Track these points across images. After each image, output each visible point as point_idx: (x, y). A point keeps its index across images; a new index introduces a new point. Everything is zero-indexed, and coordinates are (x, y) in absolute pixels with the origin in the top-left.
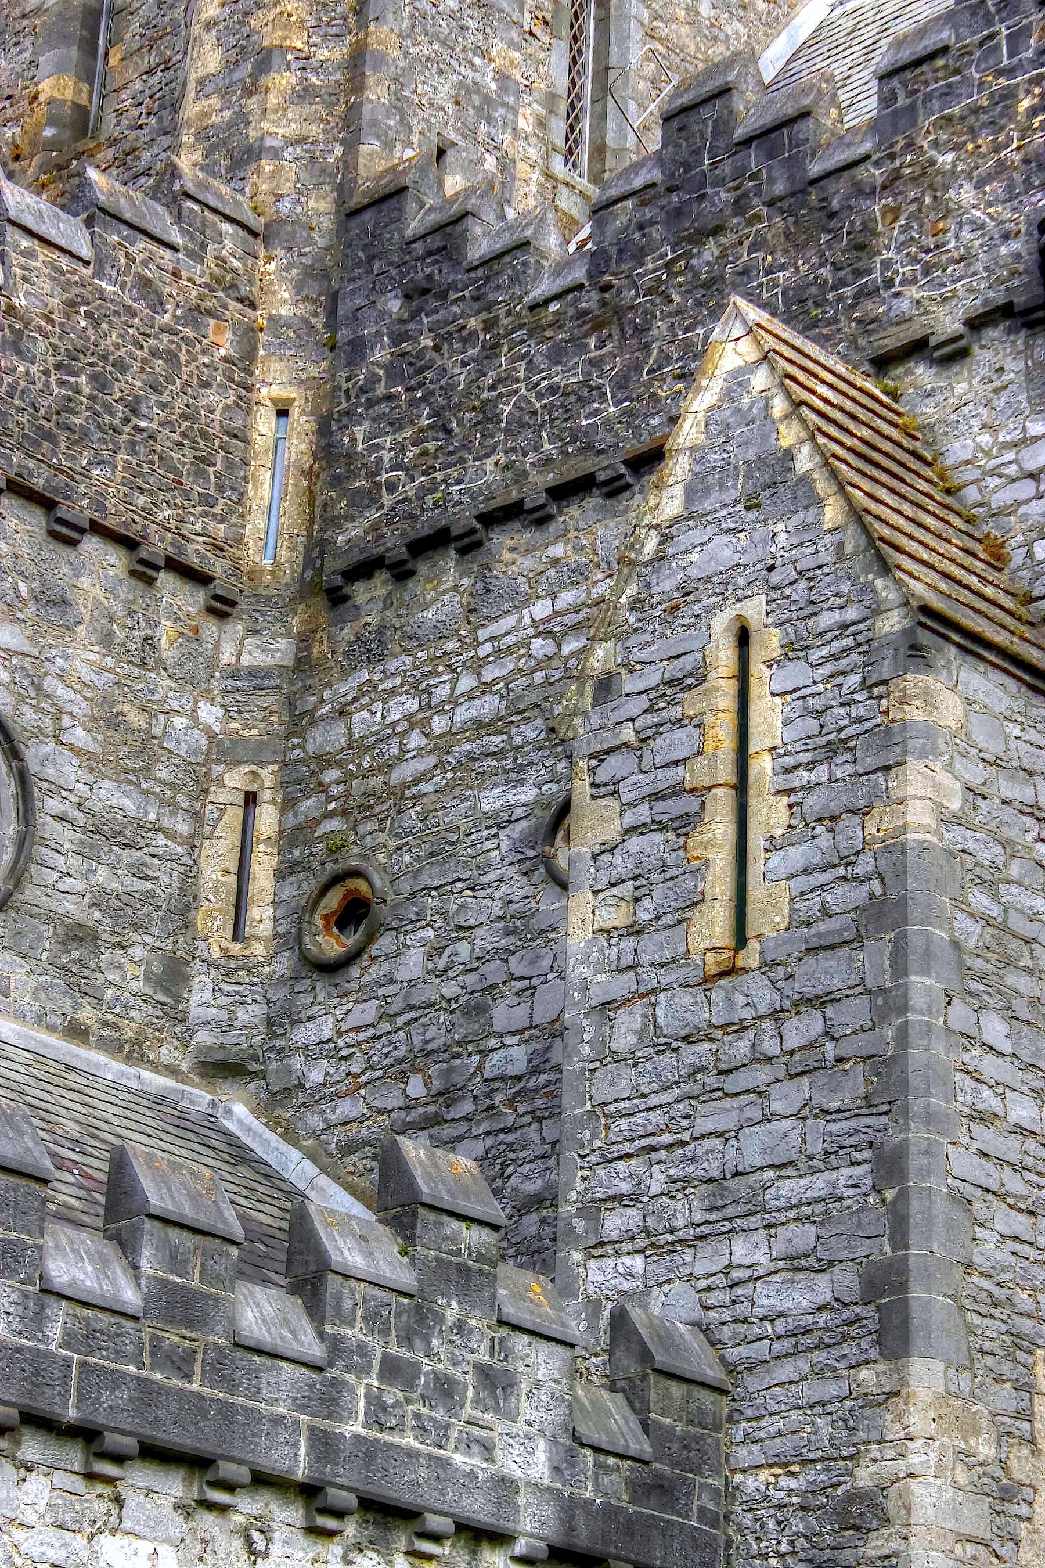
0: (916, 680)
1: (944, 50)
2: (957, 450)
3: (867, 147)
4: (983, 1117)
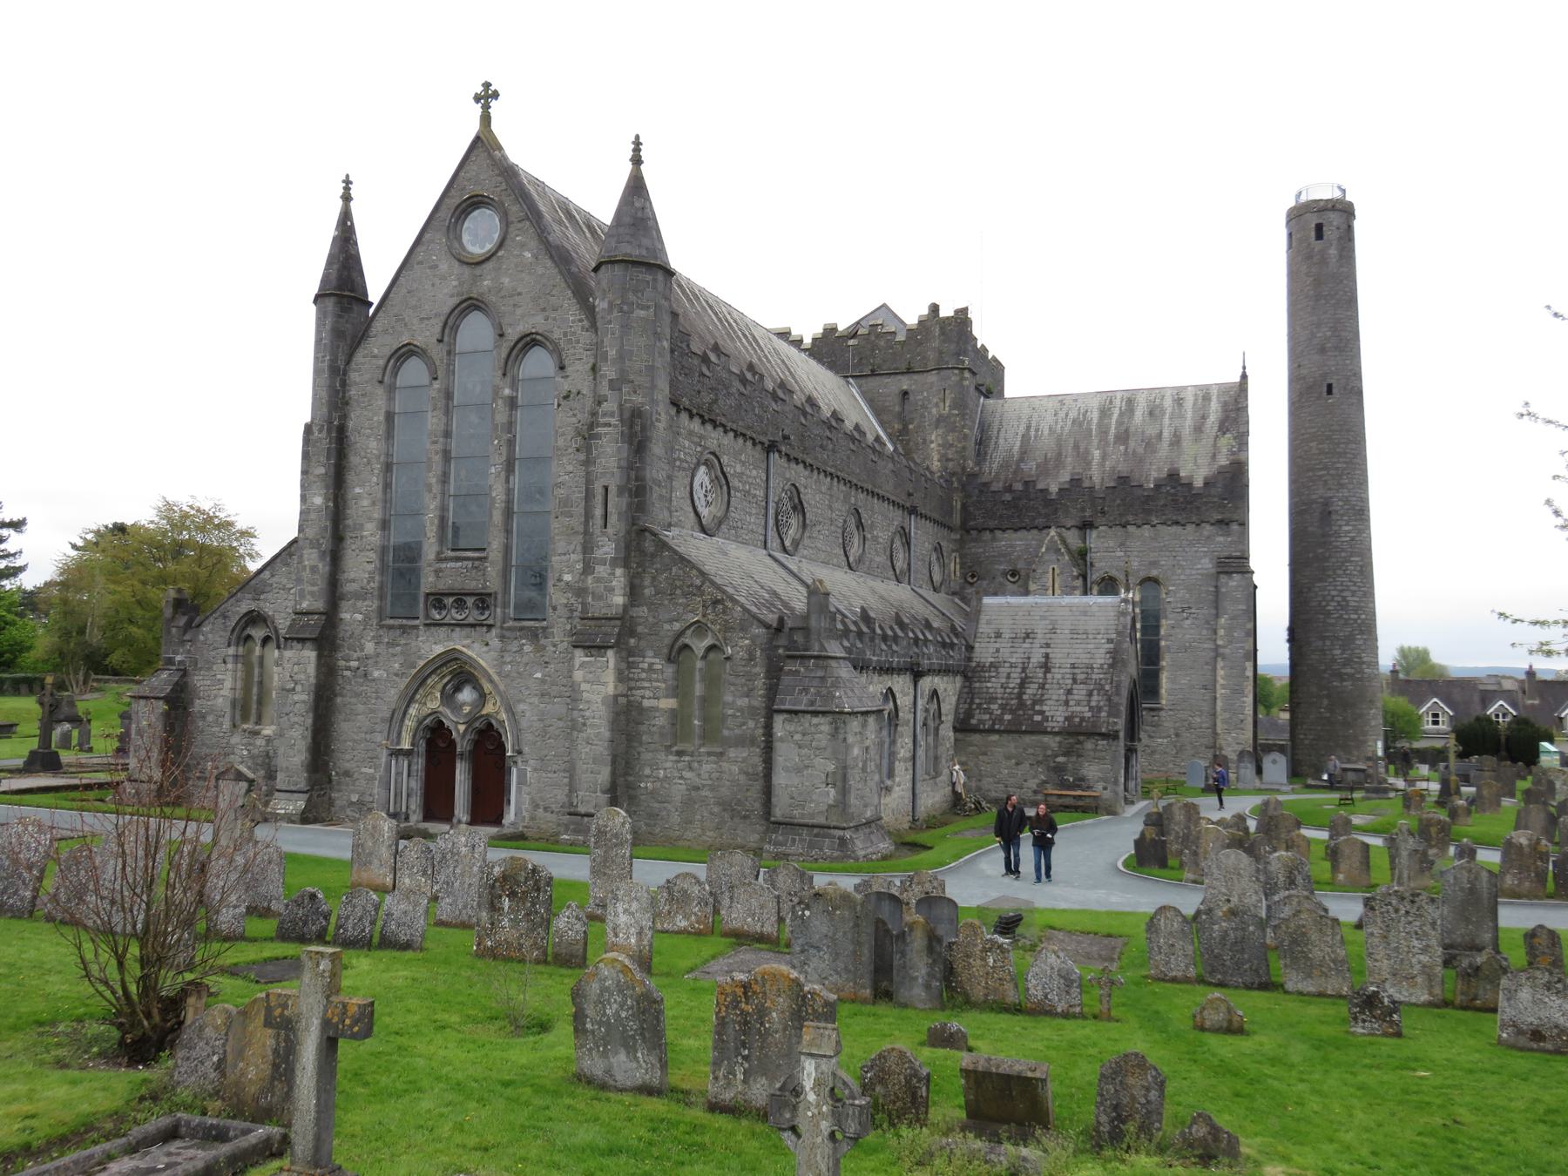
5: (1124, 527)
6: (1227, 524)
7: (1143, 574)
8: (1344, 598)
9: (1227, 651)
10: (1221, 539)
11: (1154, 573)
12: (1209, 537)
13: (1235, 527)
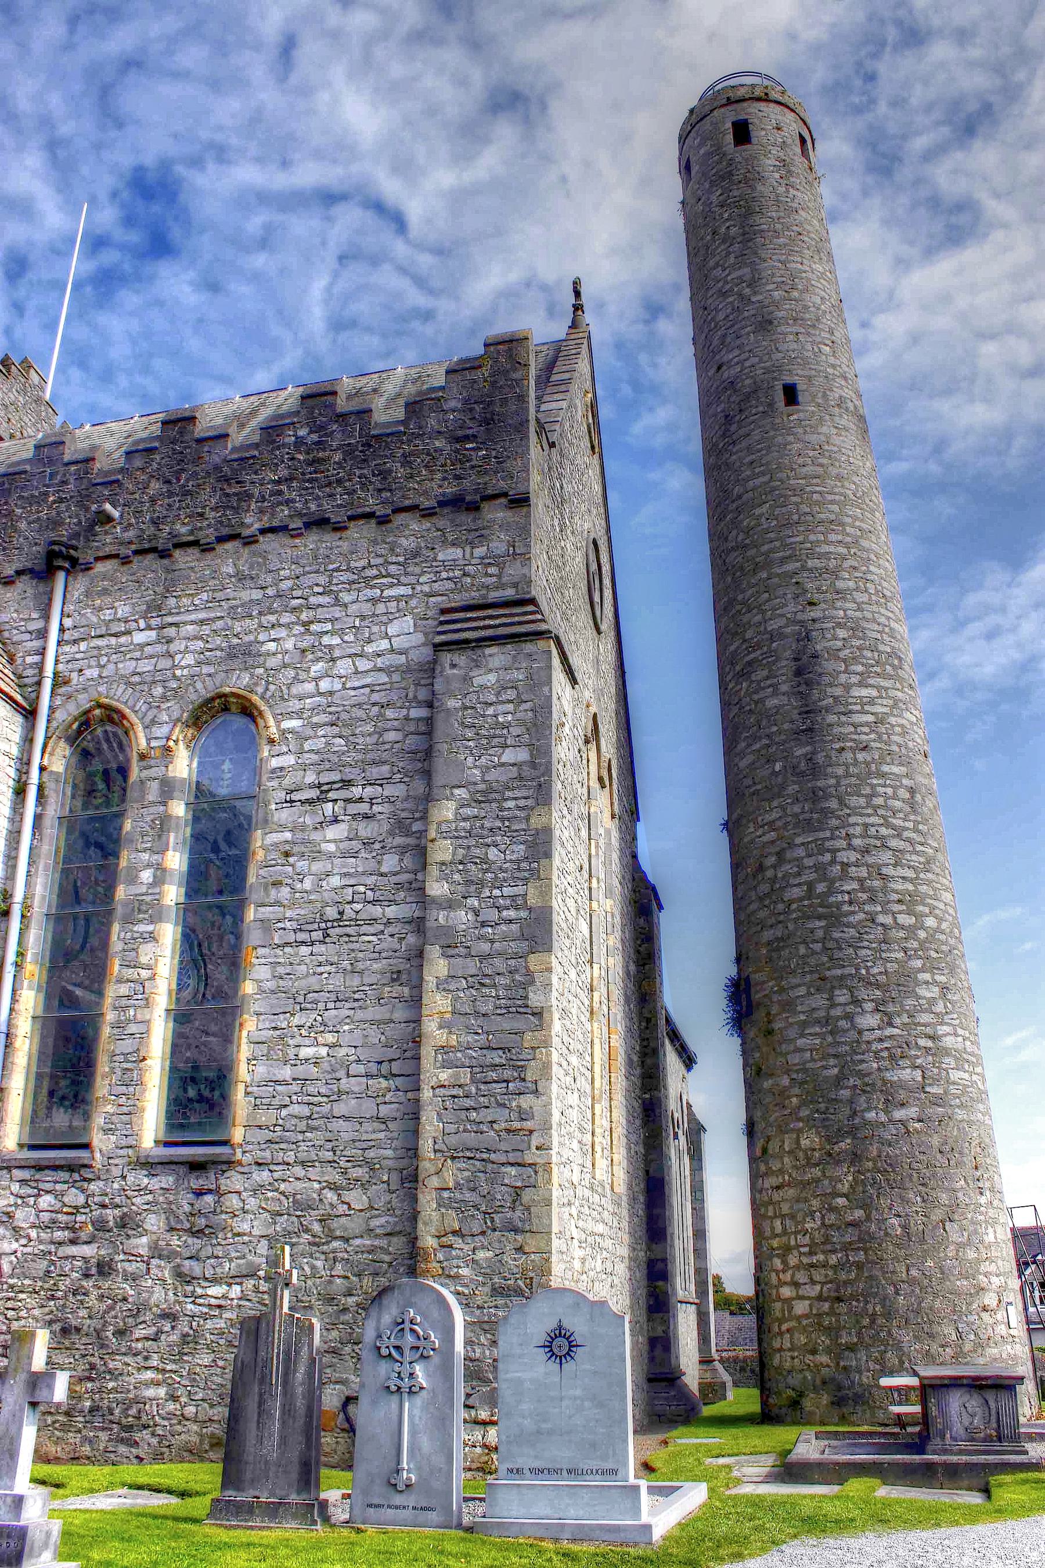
1: (25, 472)
5: (164, 554)
7: (203, 690)
9: (462, 918)
11: (238, 682)
12: (416, 554)
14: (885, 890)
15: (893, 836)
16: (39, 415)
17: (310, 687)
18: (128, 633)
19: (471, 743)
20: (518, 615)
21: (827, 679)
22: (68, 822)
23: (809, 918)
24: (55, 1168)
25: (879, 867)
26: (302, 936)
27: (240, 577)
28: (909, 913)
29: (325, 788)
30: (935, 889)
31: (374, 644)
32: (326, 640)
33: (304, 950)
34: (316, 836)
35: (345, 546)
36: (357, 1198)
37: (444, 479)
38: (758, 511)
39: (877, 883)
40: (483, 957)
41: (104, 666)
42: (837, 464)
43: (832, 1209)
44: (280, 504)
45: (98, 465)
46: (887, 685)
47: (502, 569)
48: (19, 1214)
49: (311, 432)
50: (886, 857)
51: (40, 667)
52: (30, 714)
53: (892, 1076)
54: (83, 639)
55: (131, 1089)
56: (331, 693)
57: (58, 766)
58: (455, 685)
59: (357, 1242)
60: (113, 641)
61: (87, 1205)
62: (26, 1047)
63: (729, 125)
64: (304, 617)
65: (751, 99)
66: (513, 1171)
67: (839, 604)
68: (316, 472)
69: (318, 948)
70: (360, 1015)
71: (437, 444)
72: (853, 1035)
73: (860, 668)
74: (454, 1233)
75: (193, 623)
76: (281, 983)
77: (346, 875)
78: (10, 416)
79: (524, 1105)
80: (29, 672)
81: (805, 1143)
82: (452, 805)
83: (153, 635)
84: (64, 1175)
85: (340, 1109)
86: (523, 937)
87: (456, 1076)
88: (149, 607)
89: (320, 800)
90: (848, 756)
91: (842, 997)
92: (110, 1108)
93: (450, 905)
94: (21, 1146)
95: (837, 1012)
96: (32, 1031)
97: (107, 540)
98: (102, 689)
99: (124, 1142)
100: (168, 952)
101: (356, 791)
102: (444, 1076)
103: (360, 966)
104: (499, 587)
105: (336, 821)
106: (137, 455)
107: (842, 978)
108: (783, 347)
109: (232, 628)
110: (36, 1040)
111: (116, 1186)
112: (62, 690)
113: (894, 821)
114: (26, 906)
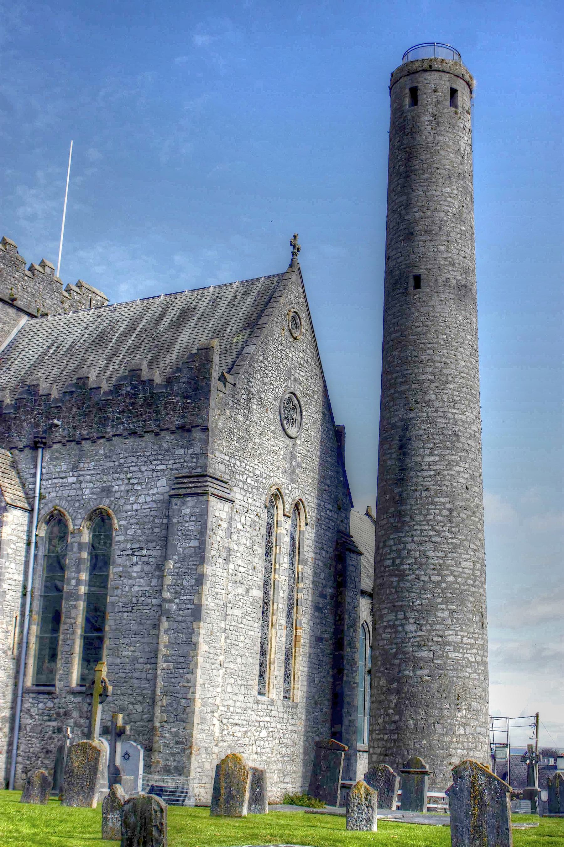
0: (5, 514)
1: (25, 398)
2: (20, 467)
3: (12, 411)
4: (10, 579)
5: (78, 443)
6: (189, 431)
7: (92, 505)
8: (424, 553)
10: (181, 451)
11: (104, 504)
12: (168, 451)
13: (197, 434)
14: (426, 564)
15: (436, 535)
16: (52, 290)
17: (129, 507)
18: (66, 477)
19: (180, 538)
20: (199, 482)
21: (413, 452)
22: (47, 557)
23: (392, 576)
24: (44, 693)
25: (426, 551)
26: (125, 609)
27: (106, 456)
28: (438, 575)
29: (134, 550)
30: (456, 562)
31: (152, 490)
32: (136, 487)
33: (125, 615)
34: (130, 570)
35: (143, 444)
36: (139, 708)
37: (178, 417)
38: (394, 353)
39: (423, 560)
40: (179, 622)
41: (57, 492)
42: (436, 324)
43: (388, 715)
44: (119, 424)
45: (53, 396)
46: (445, 453)
47: (197, 460)
48: (32, 710)
49: (132, 389)
50: (430, 546)
51: (34, 489)
52: (31, 511)
53: (418, 655)
54: (50, 479)
55: (68, 665)
56: (137, 510)
57: (42, 534)
58: (176, 513)
59: (138, 723)
60: (61, 480)
61: (54, 708)
62: (34, 647)
63: (407, 91)
64: (129, 476)
65: (420, 71)
66: (184, 701)
67: (425, 409)
68: (133, 409)
69: (130, 614)
70: (142, 640)
71: (177, 399)
72: (403, 634)
73: (431, 445)
74: (165, 721)
75: (89, 475)
76: (118, 627)
77: (139, 586)
78: (36, 299)
79: (189, 678)
80: (31, 492)
81: (381, 683)
82: (172, 562)
83: (75, 478)
84: (46, 696)
85: (135, 675)
86: (192, 615)
87: (168, 665)
88: (73, 467)
89: (133, 555)
90: (418, 494)
91: (401, 615)
92: (61, 672)
93: (170, 601)
94: (33, 685)
95: (398, 623)
96: (36, 641)
97: (57, 435)
98: (57, 502)
99: (66, 685)
100: (81, 612)
101: (144, 552)
102: (165, 665)
103: (143, 621)
104: (197, 467)
105: (137, 564)
106: (67, 394)
107: (402, 606)
108: (416, 250)
109: (102, 479)
110: (38, 645)
111: (63, 701)
112: (43, 501)
113: (437, 528)
114: (32, 592)
